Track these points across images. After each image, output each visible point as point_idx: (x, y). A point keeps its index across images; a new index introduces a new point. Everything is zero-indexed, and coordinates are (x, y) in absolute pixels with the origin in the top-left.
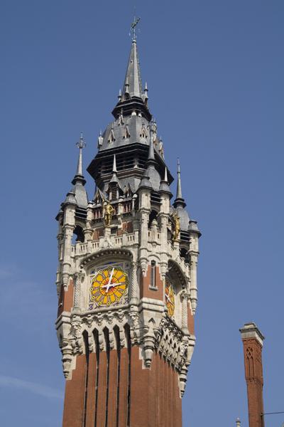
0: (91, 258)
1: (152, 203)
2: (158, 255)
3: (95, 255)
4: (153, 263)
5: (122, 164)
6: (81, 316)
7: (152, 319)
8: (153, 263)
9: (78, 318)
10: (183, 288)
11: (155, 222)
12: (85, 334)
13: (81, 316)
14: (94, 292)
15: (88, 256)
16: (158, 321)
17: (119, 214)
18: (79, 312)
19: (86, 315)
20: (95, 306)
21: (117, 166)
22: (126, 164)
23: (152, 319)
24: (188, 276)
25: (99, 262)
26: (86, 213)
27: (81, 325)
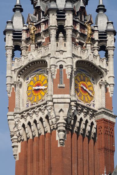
0: (24, 69)
1: (58, 20)
2: (65, 60)
3: (26, 67)
4: (61, 67)
6: (20, 114)
7: (61, 109)
8: (61, 67)
9: (18, 115)
10: (102, 78)
11: (61, 35)
12: (23, 126)
13: (20, 114)
14: (29, 94)
15: (22, 67)
16: (66, 110)
18: (18, 111)
19: (23, 113)
20: (29, 105)
23: (61, 109)
25: (31, 71)
27: (21, 120)
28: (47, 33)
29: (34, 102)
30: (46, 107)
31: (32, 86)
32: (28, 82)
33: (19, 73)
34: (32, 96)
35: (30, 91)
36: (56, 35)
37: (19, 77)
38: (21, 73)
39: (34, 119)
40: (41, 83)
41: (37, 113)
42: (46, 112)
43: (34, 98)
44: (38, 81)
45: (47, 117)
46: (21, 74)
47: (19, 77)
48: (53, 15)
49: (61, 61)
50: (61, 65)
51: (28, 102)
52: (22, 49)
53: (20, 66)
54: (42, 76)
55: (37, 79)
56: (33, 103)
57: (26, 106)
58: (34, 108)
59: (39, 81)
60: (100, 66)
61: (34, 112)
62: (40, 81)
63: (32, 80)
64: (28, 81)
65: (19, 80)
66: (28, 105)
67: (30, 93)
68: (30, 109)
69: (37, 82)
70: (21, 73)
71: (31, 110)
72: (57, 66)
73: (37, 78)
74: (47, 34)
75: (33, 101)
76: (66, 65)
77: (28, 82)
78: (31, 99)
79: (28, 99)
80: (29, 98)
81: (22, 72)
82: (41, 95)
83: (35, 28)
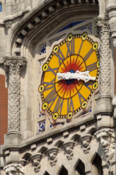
0: (31, 20)
6: (21, 150)
9: (15, 155)
13: (21, 150)
14: (46, 94)
15: (26, 16)
18: (16, 142)
19: (28, 147)
20: (47, 125)
25: (52, 27)
27: (23, 169)
29: (61, 116)
30: (93, 132)
31: (55, 71)
32: (44, 58)
33: (18, 34)
34: (54, 100)
35: (48, 84)
37: (19, 45)
38: (24, 32)
39: (60, 166)
40: (82, 61)
41: (68, 148)
42: (94, 147)
43: (62, 105)
44: (72, 57)
45: (97, 160)
46: (22, 36)
47: (19, 45)
51: (42, 118)
53: (20, 13)
54: (83, 41)
55: (69, 51)
56: (59, 121)
57: (36, 127)
58: (59, 134)
59: (76, 57)
61: (60, 145)
62: (78, 55)
63: (55, 52)
64: (43, 55)
65: (18, 54)
66: (43, 126)
67: (51, 90)
68: (49, 137)
69: (68, 59)
70: (24, 32)
71: (50, 140)
73: (68, 46)
75: (56, 114)
77: (44, 58)
78: (52, 109)
79: (44, 108)
80: (46, 104)
81: (27, 29)
82: (80, 96)
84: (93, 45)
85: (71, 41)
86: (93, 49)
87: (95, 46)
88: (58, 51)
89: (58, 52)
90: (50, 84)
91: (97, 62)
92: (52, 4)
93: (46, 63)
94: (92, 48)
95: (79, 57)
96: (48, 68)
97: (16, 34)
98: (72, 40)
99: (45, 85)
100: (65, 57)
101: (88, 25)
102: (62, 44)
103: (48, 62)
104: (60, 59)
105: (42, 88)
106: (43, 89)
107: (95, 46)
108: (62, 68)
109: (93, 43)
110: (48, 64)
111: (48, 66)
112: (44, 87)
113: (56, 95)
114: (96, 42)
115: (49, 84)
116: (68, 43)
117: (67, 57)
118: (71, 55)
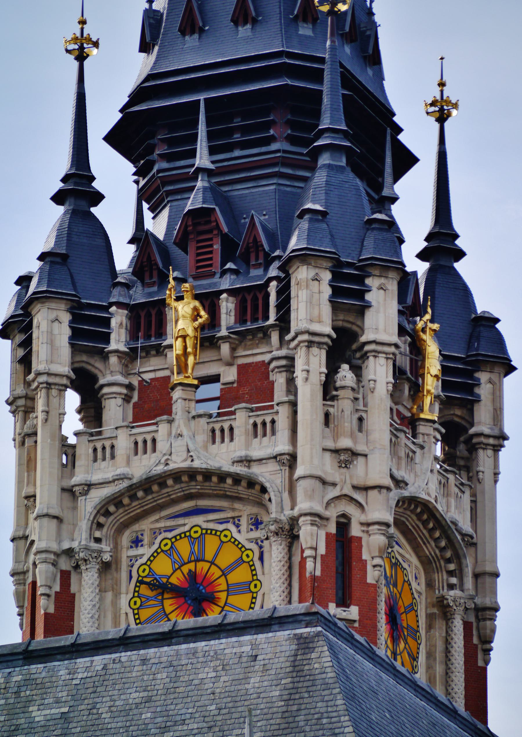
1: (335, 307)
5: (230, 132)
17: (224, 332)
21: (211, 136)
22: (245, 130)
24: (466, 526)
26: (106, 323)
28: (249, 343)
36: (327, 376)
40: (218, 573)
44: (200, 565)
48: (316, 279)
49: (346, 495)
50: (344, 516)
52: (105, 390)
54: (222, 542)
55: (192, 553)
59: (206, 566)
60: (455, 524)
63: (165, 549)
69: (192, 566)
72: (327, 519)
73: (192, 544)
74: (245, 349)
76: (363, 518)
83: (199, 315)
84: (243, 552)
85: (198, 538)
86: (242, 559)
87: (248, 556)
88: (172, 547)
89: (169, 549)
90: (151, 599)
91: (251, 582)
92: (173, 476)
93: (145, 564)
94: (241, 557)
95: (213, 566)
96: (150, 571)
97: (98, 512)
98: (200, 537)
99: (143, 600)
100: (186, 561)
101: (233, 518)
102: (178, 537)
103: (149, 563)
104: (173, 563)
105: (135, 603)
106: (139, 603)
107: (248, 556)
108: (178, 579)
109: (243, 549)
110: (149, 566)
111: (150, 568)
112: (141, 602)
113: (166, 619)
114: (251, 550)
115: (151, 599)
116: (192, 540)
117: (189, 562)
118: (197, 560)
